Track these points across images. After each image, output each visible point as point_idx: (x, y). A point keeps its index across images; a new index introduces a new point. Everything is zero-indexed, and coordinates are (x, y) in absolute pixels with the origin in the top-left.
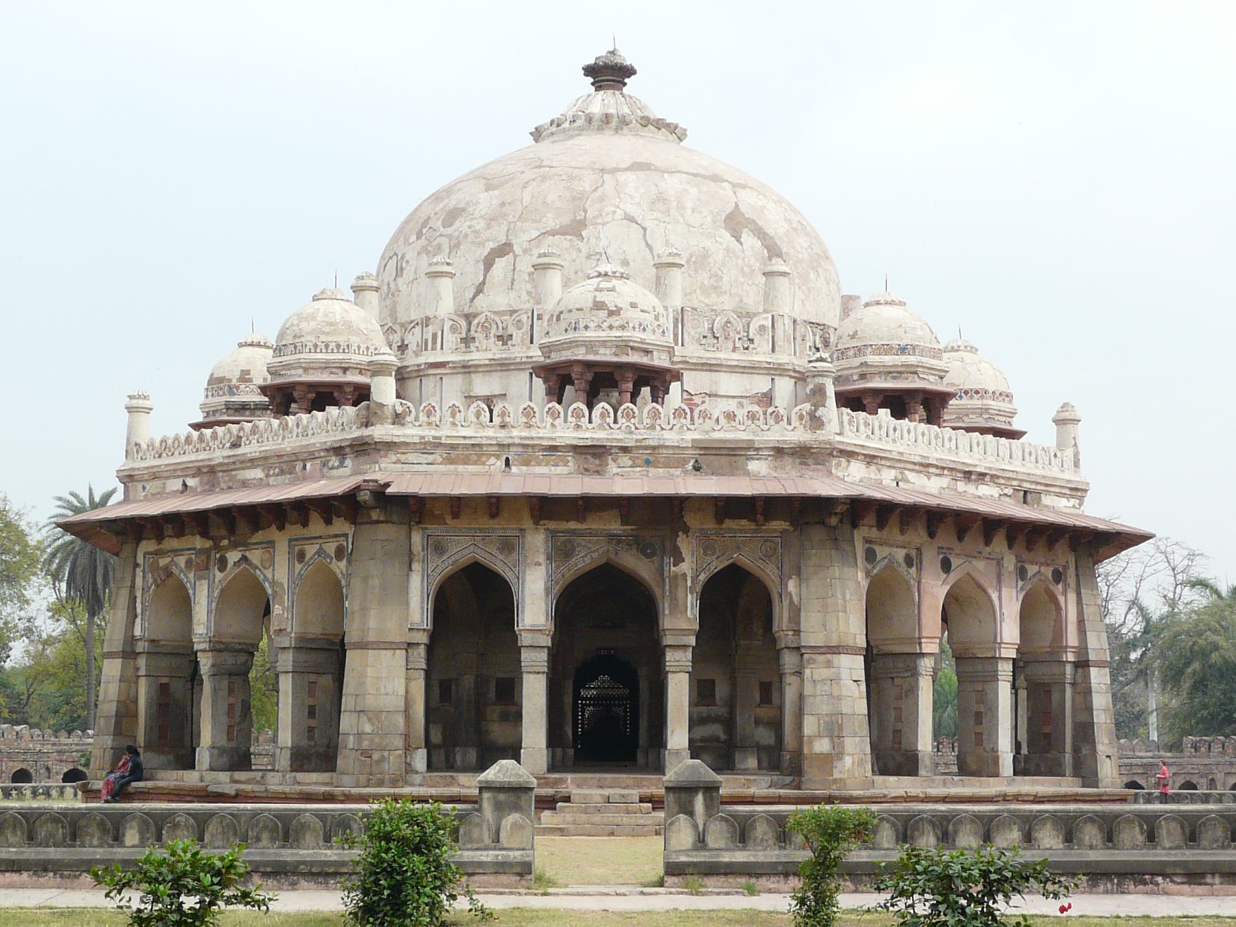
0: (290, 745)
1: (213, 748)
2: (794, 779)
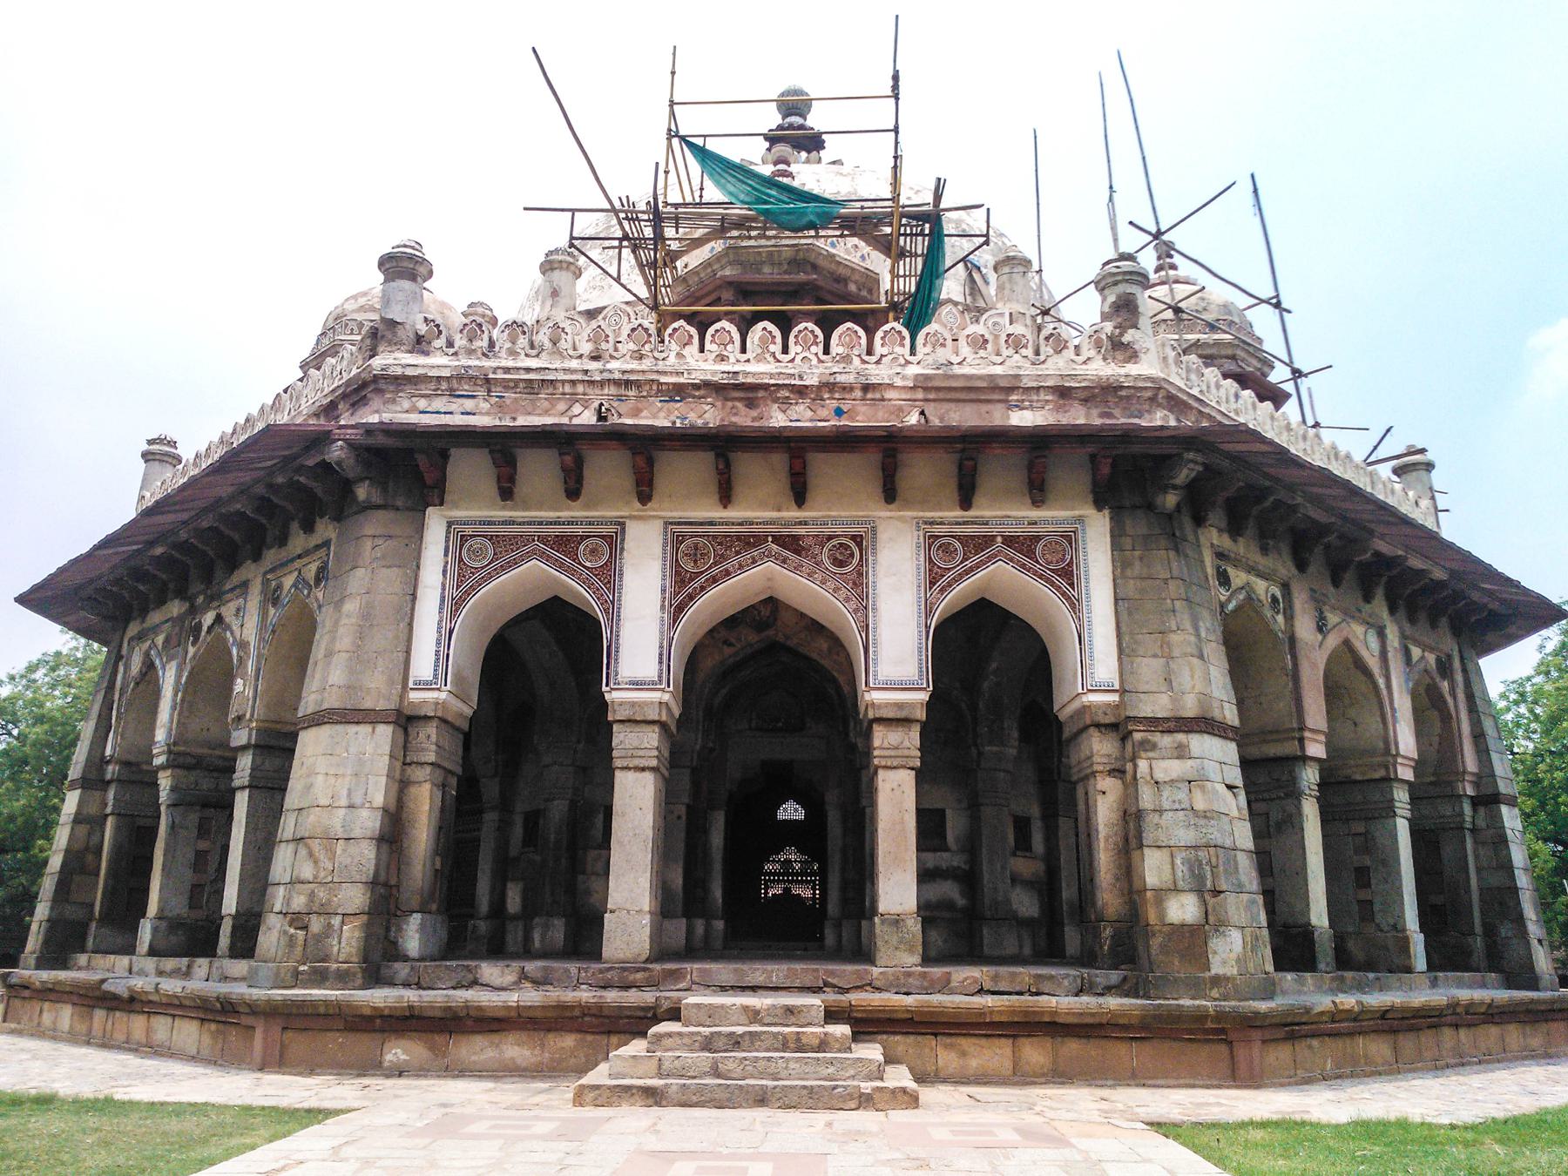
0: (233, 911)
1: (159, 918)
2: (1125, 979)
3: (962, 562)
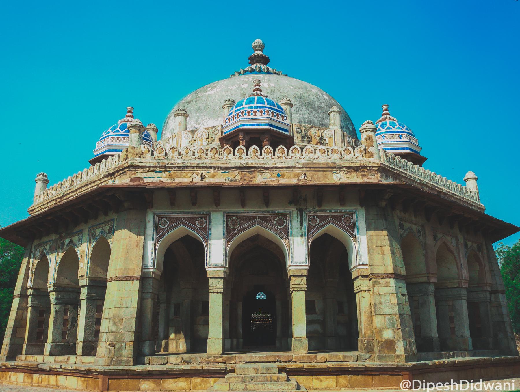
1: (53, 343)
3: (318, 224)
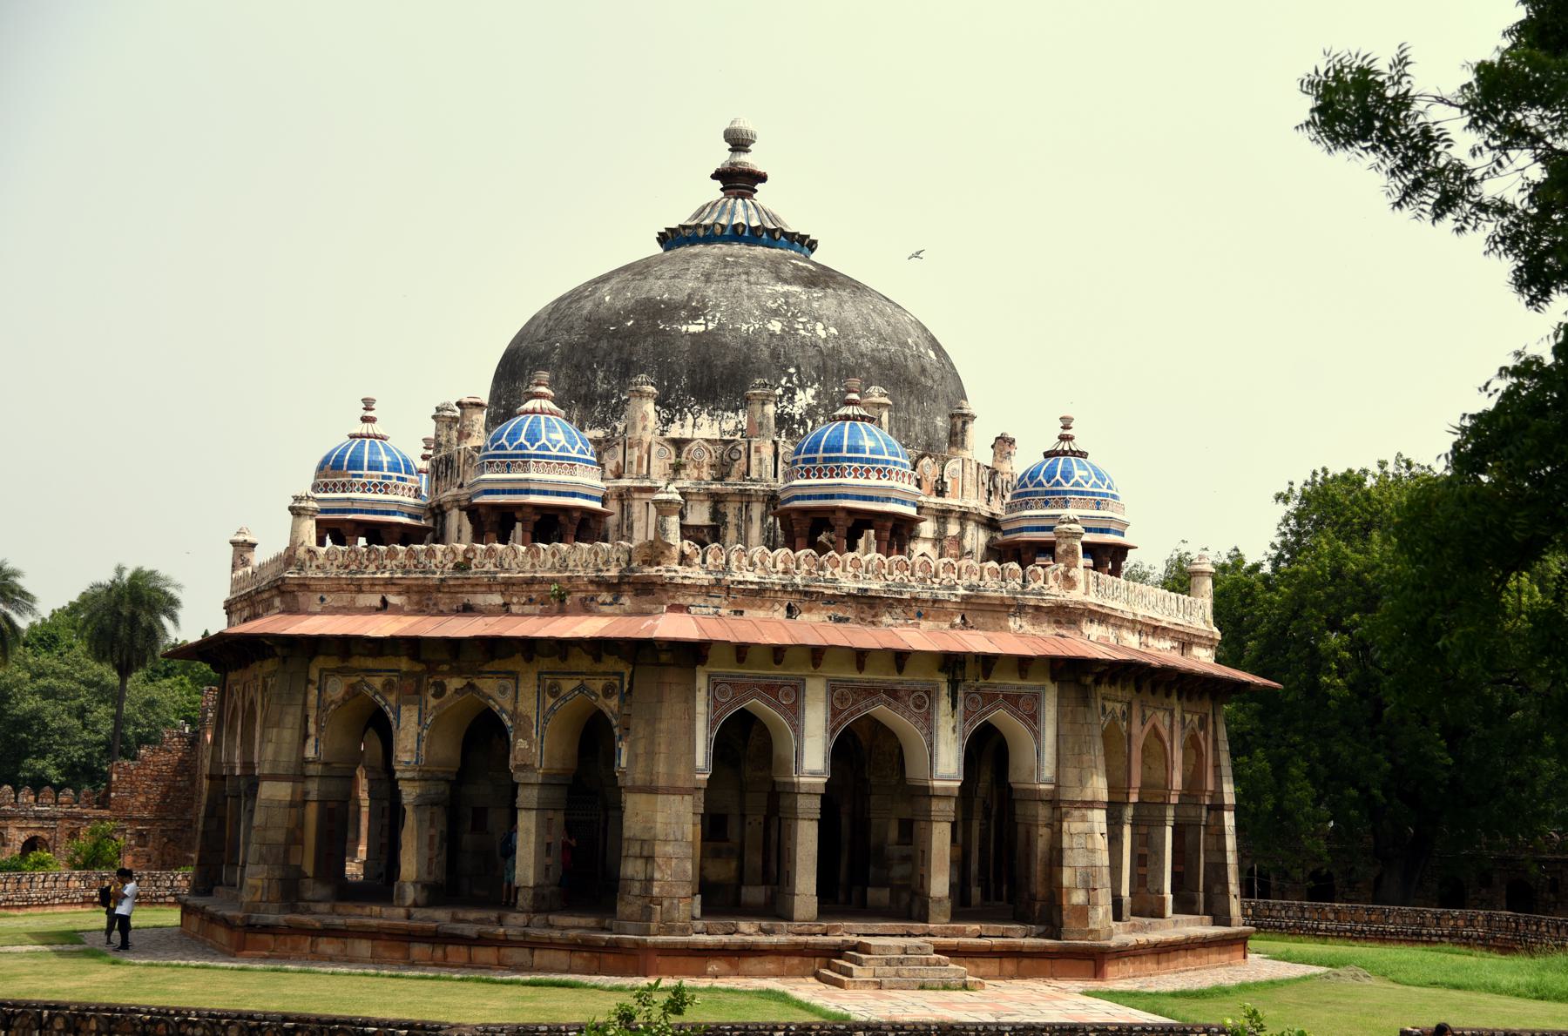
0: (531, 884)
